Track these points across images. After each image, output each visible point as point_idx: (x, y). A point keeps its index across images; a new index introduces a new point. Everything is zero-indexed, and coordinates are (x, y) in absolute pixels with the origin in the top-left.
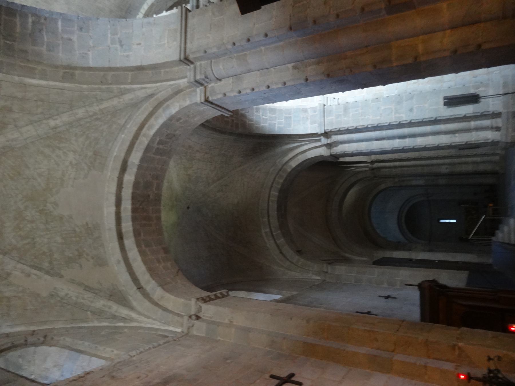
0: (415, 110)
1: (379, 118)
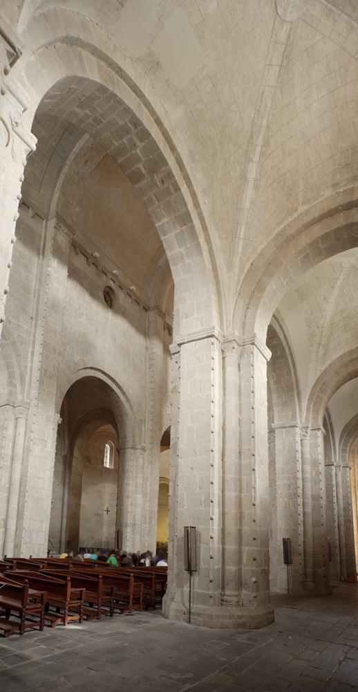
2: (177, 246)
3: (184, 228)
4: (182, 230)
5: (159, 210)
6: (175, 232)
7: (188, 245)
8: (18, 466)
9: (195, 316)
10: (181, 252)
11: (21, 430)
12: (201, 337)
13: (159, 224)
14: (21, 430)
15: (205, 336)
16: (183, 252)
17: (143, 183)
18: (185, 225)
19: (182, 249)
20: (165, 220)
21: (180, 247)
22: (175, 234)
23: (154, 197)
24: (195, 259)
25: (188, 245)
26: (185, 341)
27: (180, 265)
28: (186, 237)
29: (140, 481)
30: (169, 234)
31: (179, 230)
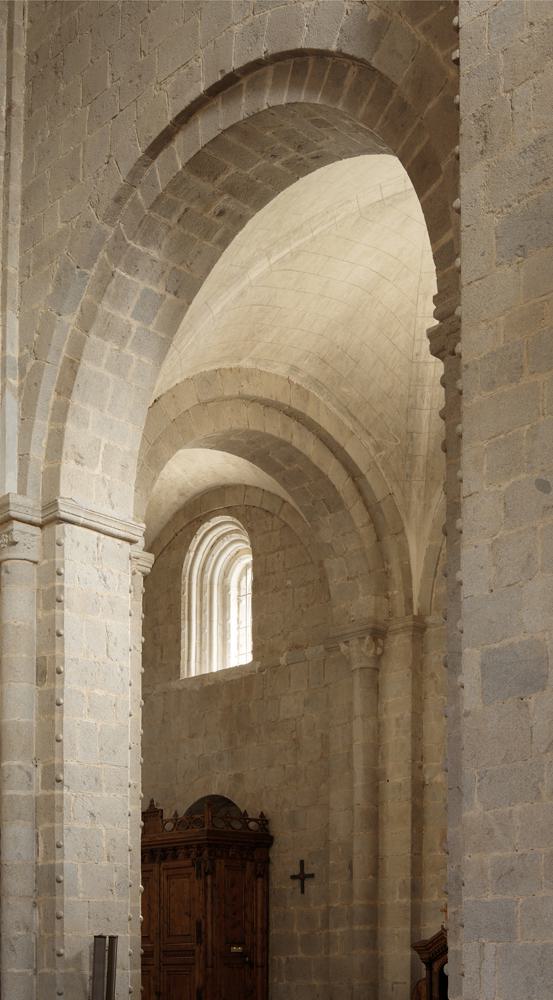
2: (131, 310)
3: (170, 297)
4: (163, 297)
5: (163, 231)
6: (150, 287)
7: (151, 328)
9: (98, 471)
10: (130, 326)
12: (116, 532)
13: (140, 248)
15: (122, 534)
16: (134, 330)
17: (207, 186)
18: (175, 293)
19: (136, 324)
20: (154, 253)
21: (135, 315)
22: (146, 293)
23: (182, 210)
24: (144, 359)
25: (151, 328)
26: (81, 520)
27: (110, 346)
28: (160, 312)
30: (136, 280)
31: (158, 289)
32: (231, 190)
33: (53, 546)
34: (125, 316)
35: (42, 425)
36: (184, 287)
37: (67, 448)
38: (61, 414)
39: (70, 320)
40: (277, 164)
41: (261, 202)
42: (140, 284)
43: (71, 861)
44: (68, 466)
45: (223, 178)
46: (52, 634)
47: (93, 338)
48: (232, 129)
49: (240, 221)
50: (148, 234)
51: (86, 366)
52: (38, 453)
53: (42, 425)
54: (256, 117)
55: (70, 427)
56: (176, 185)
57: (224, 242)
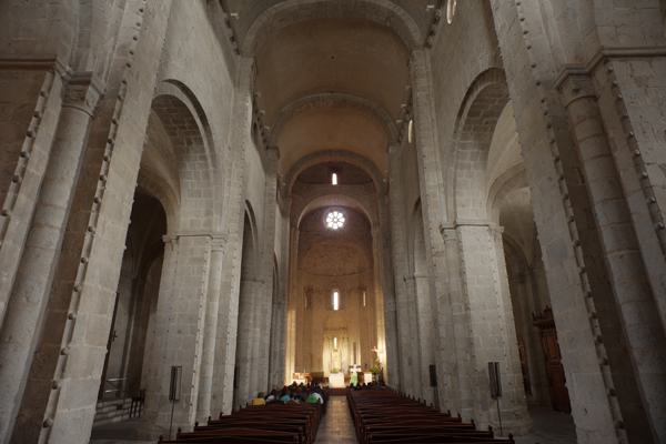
0: (178, 336)
1: (180, 296)
8: (216, 304)
11: (220, 264)
14: (220, 264)
19: (472, 163)
27: (465, 171)
29: (259, 314)
31: (476, 150)
32: (485, 116)
33: (458, 234)
34: (467, 161)
35: (451, 199)
36: (485, 147)
37: (458, 203)
38: (454, 196)
39: (452, 168)
40: (496, 103)
41: (498, 115)
42: (469, 151)
43: (476, 335)
44: (459, 209)
45: (482, 114)
46: (461, 261)
47: (459, 171)
48: (475, 101)
49: (495, 122)
50: (464, 137)
51: (458, 179)
52: (451, 207)
53: (451, 199)
54: (479, 96)
55: (457, 198)
56: (467, 121)
57: (493, 130)
